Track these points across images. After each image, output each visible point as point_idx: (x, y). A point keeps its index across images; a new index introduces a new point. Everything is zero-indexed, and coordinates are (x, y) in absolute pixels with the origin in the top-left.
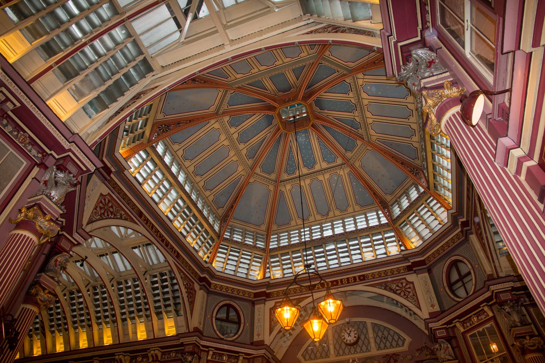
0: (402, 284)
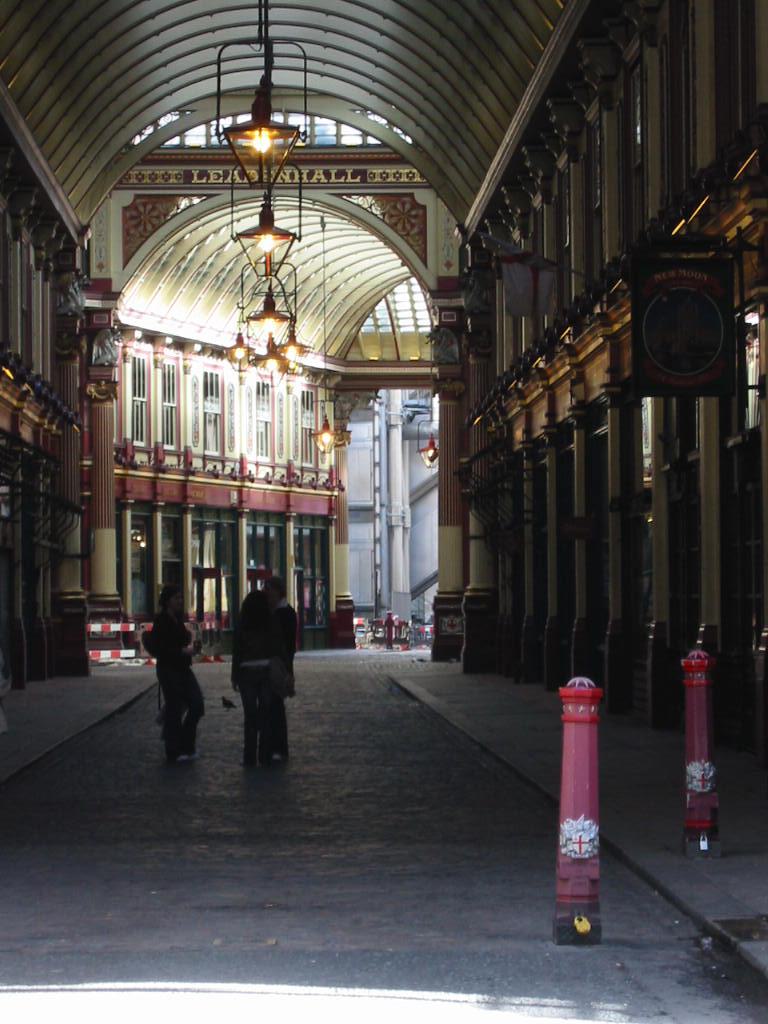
0: (403, 204)
